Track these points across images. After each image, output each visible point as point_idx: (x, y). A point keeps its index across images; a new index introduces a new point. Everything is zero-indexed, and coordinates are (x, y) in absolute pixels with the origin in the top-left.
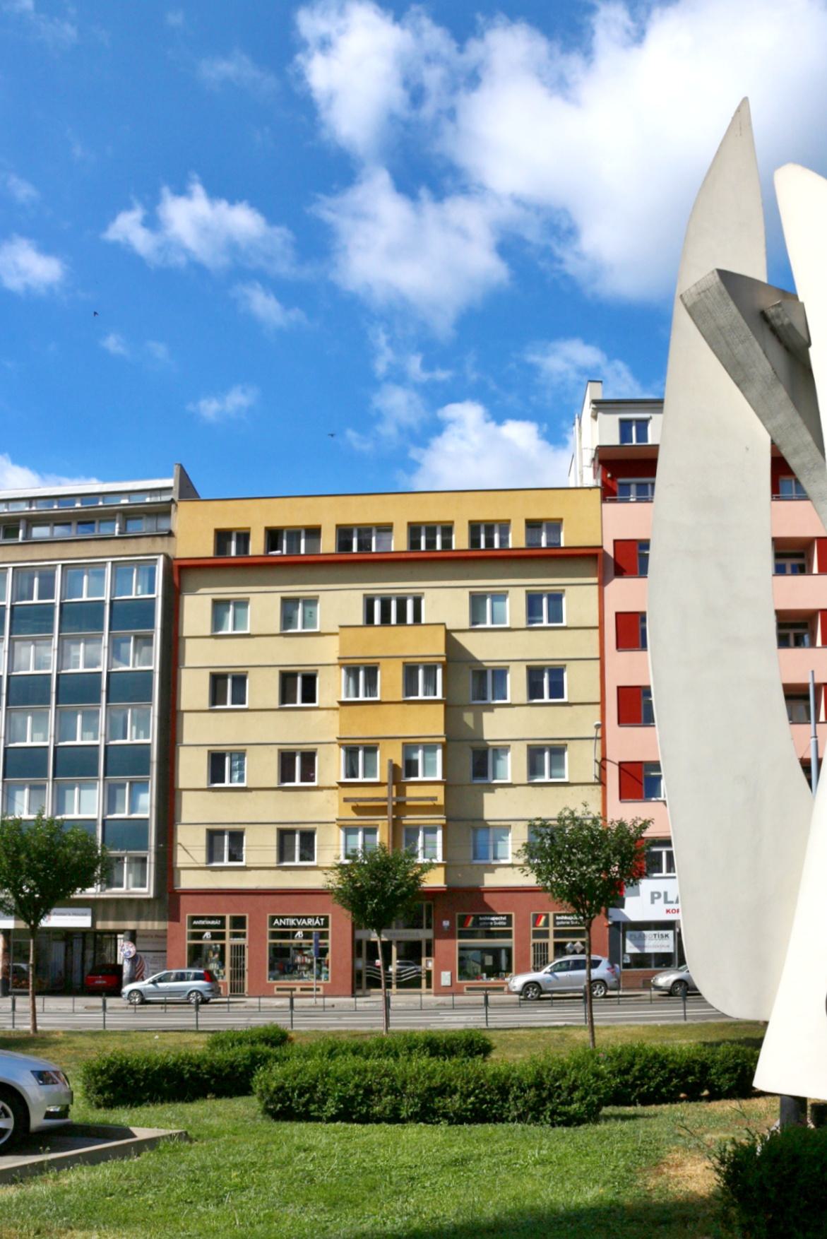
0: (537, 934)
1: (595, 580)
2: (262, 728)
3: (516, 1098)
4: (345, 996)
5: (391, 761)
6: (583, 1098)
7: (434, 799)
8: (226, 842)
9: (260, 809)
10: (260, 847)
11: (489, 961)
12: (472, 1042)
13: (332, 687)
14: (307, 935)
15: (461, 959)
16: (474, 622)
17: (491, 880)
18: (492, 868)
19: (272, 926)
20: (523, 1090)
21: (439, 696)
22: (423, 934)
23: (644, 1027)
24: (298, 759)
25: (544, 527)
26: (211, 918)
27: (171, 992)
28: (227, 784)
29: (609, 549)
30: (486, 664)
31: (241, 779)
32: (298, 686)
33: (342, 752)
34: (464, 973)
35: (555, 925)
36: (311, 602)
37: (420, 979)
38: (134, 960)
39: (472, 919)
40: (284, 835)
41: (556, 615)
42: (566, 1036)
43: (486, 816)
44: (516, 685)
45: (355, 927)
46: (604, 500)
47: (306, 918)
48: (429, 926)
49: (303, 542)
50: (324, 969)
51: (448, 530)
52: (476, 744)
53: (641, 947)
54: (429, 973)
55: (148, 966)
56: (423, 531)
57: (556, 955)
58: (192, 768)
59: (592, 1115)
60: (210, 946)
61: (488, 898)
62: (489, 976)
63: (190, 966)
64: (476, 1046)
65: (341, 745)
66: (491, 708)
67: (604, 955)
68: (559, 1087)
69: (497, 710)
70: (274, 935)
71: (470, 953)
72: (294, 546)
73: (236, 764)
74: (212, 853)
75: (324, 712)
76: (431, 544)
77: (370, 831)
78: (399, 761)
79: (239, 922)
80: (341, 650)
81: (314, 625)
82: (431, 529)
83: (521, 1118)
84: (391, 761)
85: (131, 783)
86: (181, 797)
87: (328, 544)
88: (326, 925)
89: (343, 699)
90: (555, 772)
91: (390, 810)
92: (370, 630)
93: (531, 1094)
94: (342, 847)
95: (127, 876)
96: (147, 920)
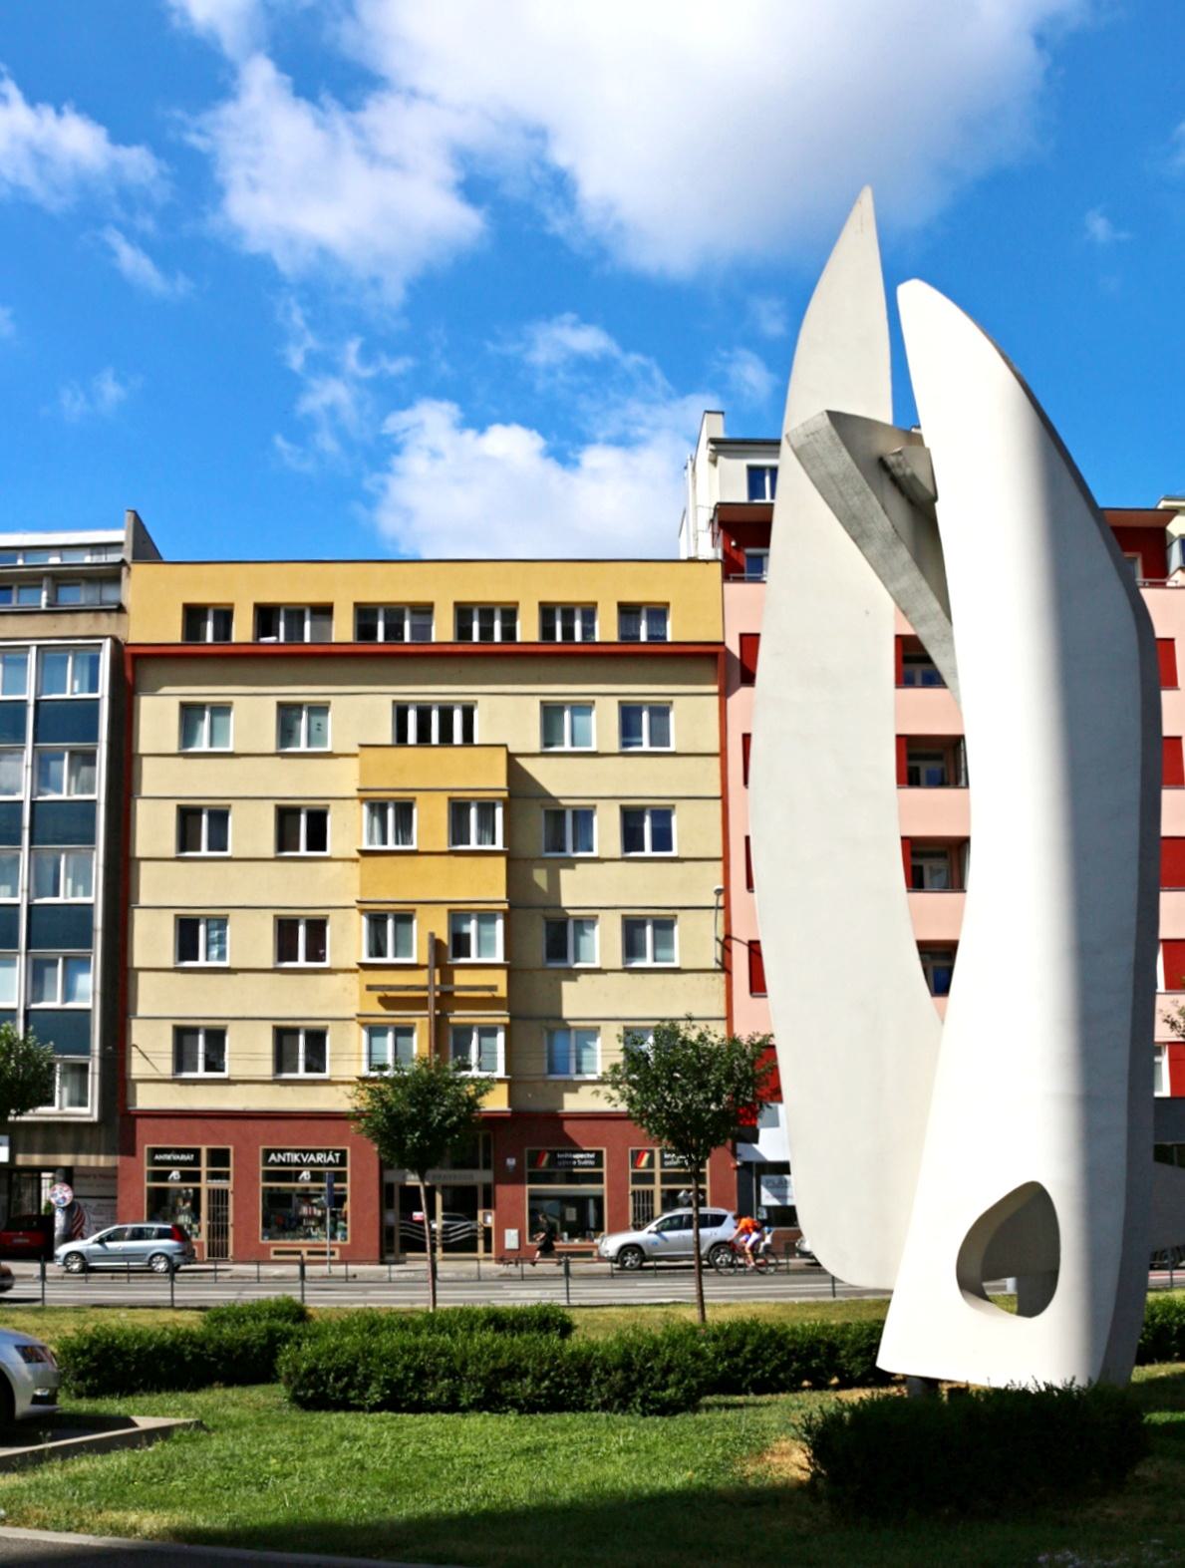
0: (640, 1178)
1: (715, 688)
2: (251, 885)
3: (600, 1382)
4: (371, 1262)
5: (432, 935)
6: (679, 1382)
7: (493, 988)
8: (200, 1045)
9: (250, 1000)
10: (249, 1051)
11: (571, 1214)
12: (547, 1319)
13: (349, 829)
14: (316, 1177)
15: (533, 1213)
16: (547, 744)
17: (572, 1103)
18: (574, 1087)
19: (266, 1163)
20: (608, 1373)
21: (499, 846)
22: (481, 1177)
23: (776, 1304)
24: (302, 930)
25: (644, 614)
26: (179, 1151)
27: (125, 1256)
28: (201, 962)
29: (734, 646)
30: (564, 802)
31: (222, 955)
32: (301, 828)
33: (364, 921)
35: (663, 1166)
36: (320, 709)
37: (474, 1240)
38: (69, 1210)
39: (547, 1157)
40: (284, 1036)
41: (660, 736)
42: (672, 1315)
43: (567, 1013)
44: (606, 832)
45: (384, 1166)
46: (726, 577)
47: (315, 1152)
48: (487, 1166)
49: (307, 625)
51: (510, 613)
52: (552, 913)
53: (783, 1197)
54: (488, 1231)
55: (90, 1218)
56: (476, 614)
57: (666, 1207)
58: (152, 939)
59: (689, 1403)
60: (179, 1191)
61: (568, 1127)
62: (571, 1236)
63: (151, 1218)
64: (554, 1322)
65: (362, 912)
66: (571, 863)
67: (728, 1209)
68: (651, 1368)
69: (580, 867)
70: (269, 1176)
71: (546, 1204)
72: (295, 632)
73: (215, 934)
75: (339, 865)
76: (486, 633)
77: (404, 1032)
78: (443, 935)
79: (219, 1157)
81: (323, 741)
82: (487, 612)
83: (605, 1406)
84: (432, 935)
85: (66, 959)
86: (136, 978)
87: (343, 629)
88: (343, 1162)
89: (366, 846)
90: (660, 953)
91: (431, 1003)
92: (403, 751)
93: (619, 1375)
94: (365, 1057)
95: (61, 1091)
96: (89, 1153)
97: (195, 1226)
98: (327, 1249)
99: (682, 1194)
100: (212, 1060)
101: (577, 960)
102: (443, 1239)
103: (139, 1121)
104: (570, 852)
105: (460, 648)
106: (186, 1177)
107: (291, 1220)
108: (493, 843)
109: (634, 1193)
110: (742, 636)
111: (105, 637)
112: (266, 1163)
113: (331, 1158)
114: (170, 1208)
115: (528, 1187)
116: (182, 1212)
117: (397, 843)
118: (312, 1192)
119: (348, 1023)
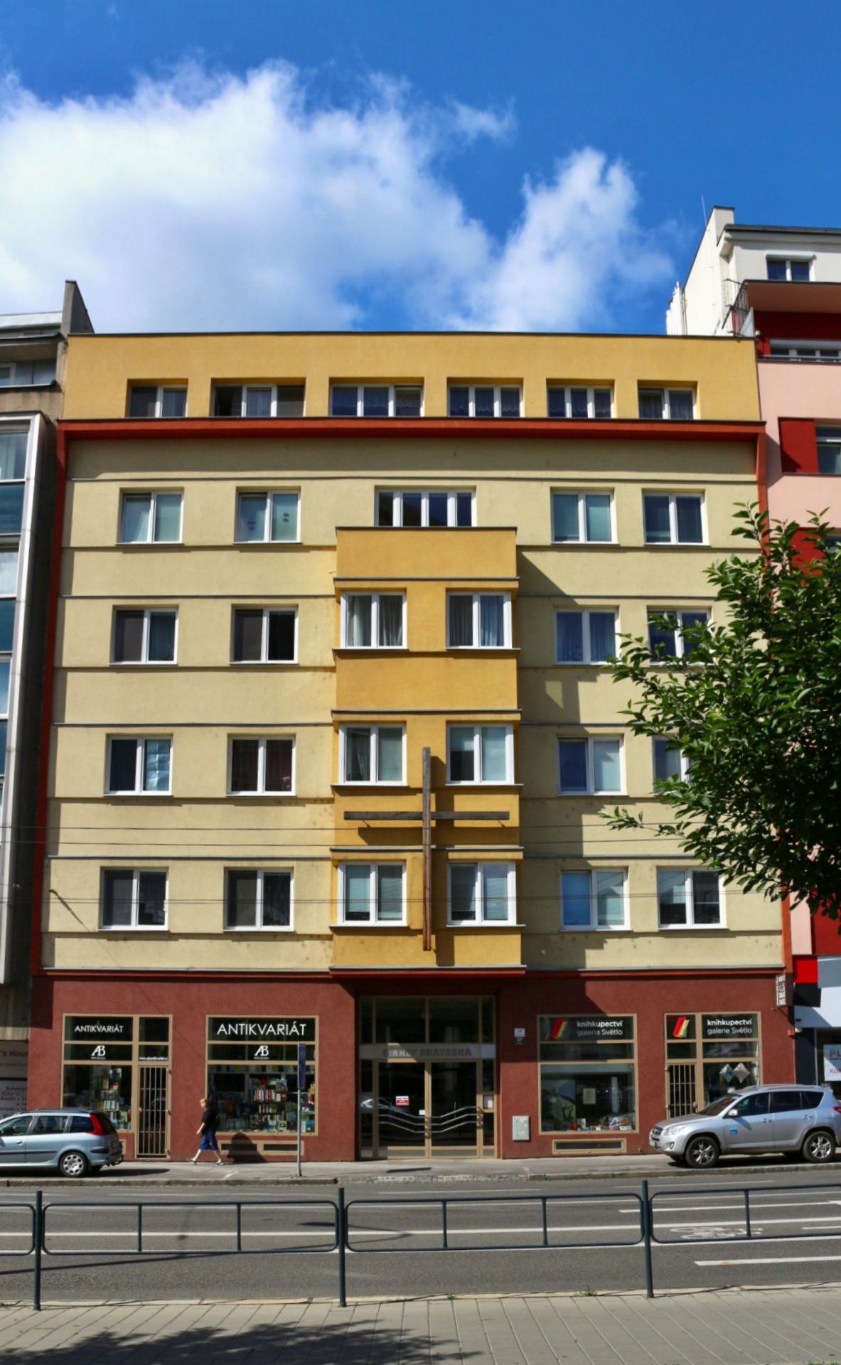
1: (754, 478)
2: (202, 699)
5: (427, 750)
7: (505, 816)
8: (133, 891)
9: (195, 837)
10: (195, 900)
11: (590, 1096)
13: (322, 631)
14: (275, 1053)
16: (558, 536)
17: (595, 960)
18: (598, 940)
24: (261, 752)
28: (138, 791)
29: (772, 431)
30: (580, 602)
31: (163, 783)
32: (264, 633)
34: (550, 1118)
35: (705, 1035)
36: (289, 497)
43: (588, 850)
45: (363, 1035)
47: (275, 1022)
48: (487, 1040)
52: (568, 732)
54: (488, 1118)
60: (105, 1069)
61: (592, 989)
62: (592, 1122)
63: (69, 1103)
66: (591, 674)
70: (216, 1052)
73: (155, 759)
74: (111, 907)
75: (308, 674)
77: (391, 872)
78: (441, 752)
79: (155, 1029)
80: (340, 565)
86: (59, 809)
87: (316, 404)
88: (310, 1035)
89: (343, 646)
91: (427, 837)
97: (124, 1114)
99: (725, 1070)
100: (147, 911)
101: (597, 790)
102: (433, 1128)
103: (57, 985)
104: (587, 660)
105: (457, 425)
106: (112, 1053)
107: (243, 1106)
108: (500, 642)
109: (671, 1069)
110: (781, 420)
111: (34, 413)
112: (213, 1035)
113: (294, 1029)
114: (93, 1092)
116: (107, 1097)
117: (381, 644)
118: (269, 1071)
119: (315, 863)
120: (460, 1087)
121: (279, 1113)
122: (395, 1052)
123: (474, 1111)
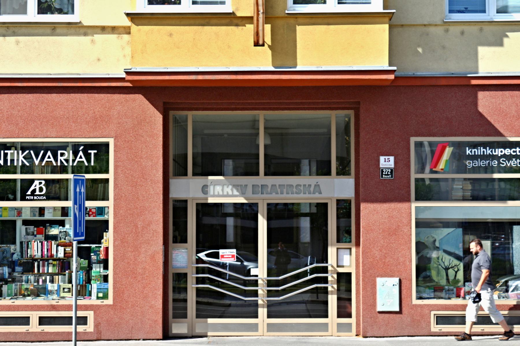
39: (448, 151)
45: (175, 166)
48: (343, 171)
50: (97, 270)
54: (344, 279)
61: (486, 102)
98: (72, 314)
102: (270, 293)
113: (81, 157)
115: (414, 205)
118: (48, 216)
120: (299, 237)
121: (61, 272)
122: (218, 189)
123: (325, 270)
